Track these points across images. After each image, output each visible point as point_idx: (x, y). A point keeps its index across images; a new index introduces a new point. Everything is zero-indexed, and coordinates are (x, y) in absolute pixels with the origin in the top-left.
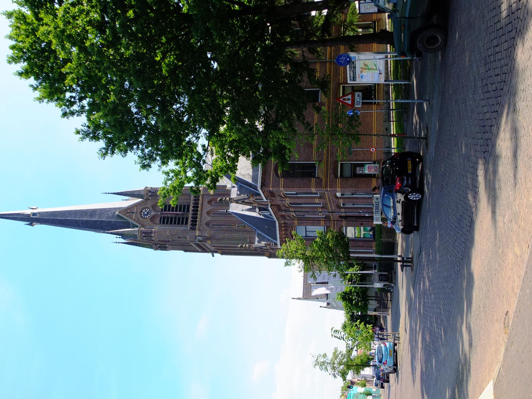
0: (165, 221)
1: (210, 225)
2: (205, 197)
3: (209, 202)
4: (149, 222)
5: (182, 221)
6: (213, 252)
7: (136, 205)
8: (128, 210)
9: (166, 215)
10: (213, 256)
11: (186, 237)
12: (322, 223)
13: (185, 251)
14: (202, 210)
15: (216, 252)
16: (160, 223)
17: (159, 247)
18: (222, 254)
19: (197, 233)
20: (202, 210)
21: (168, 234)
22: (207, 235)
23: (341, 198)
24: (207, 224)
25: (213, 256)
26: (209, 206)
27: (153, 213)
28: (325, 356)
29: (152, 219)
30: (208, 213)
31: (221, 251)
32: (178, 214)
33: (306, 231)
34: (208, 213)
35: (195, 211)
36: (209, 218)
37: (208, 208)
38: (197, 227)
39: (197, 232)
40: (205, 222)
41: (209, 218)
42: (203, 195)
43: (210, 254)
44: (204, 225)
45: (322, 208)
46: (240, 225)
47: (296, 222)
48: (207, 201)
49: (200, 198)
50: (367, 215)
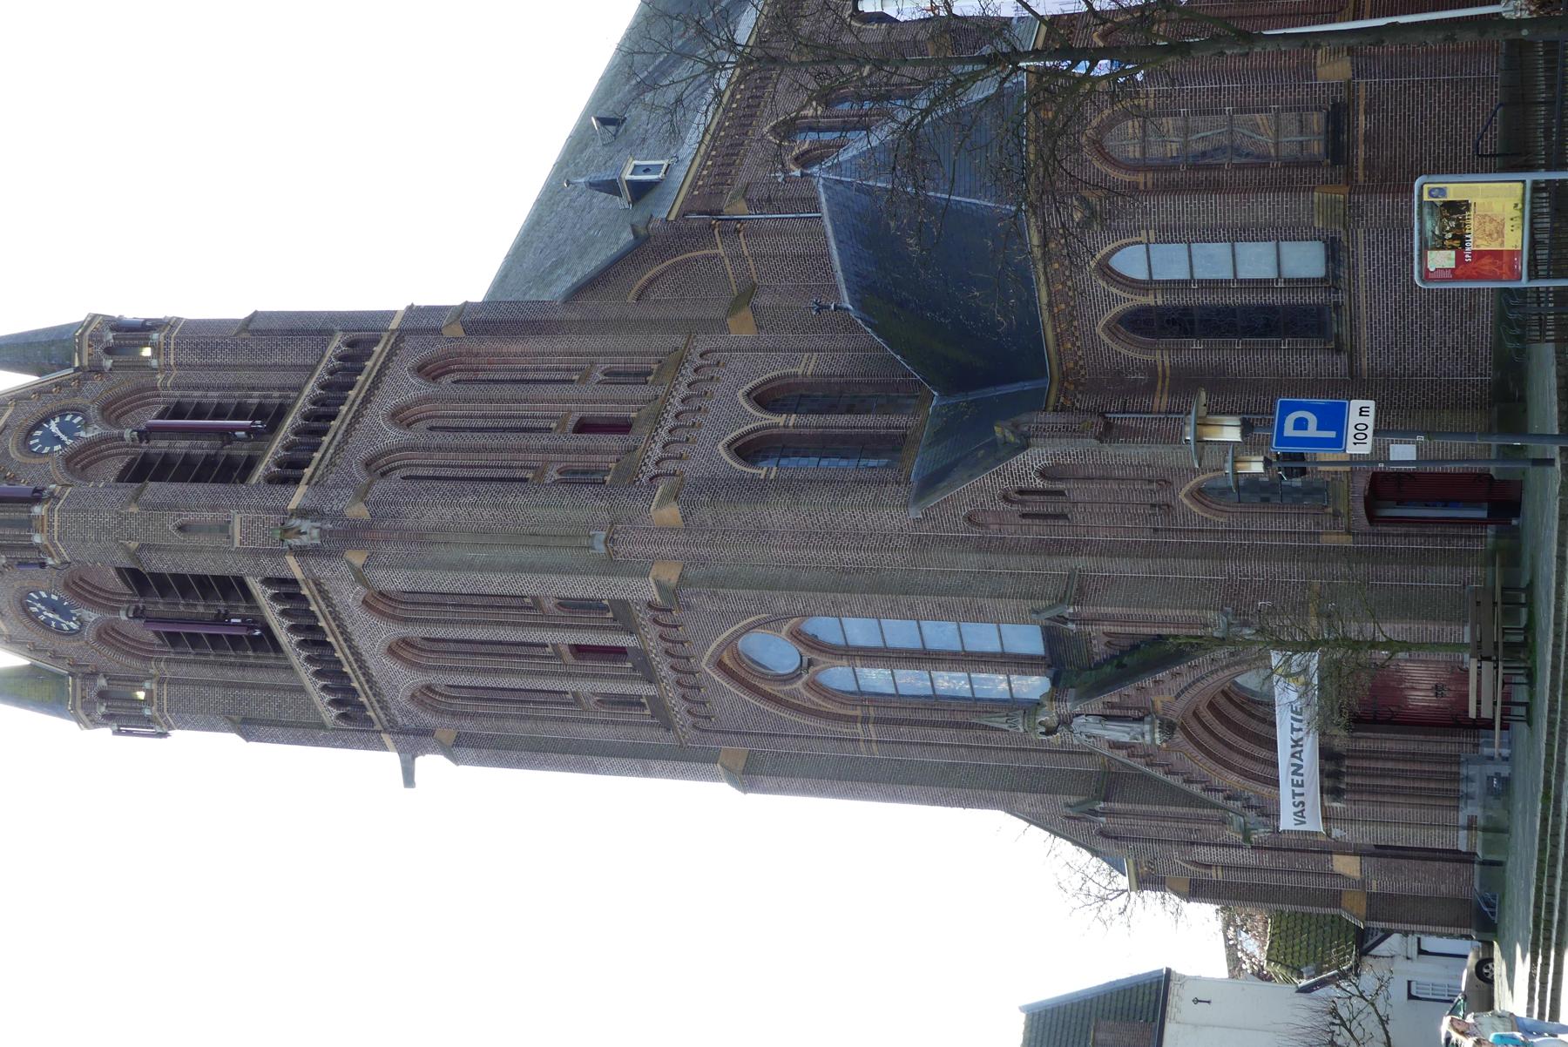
2: (410, 342)
3: (428, 371)
4: (55, 468)
10: (409, 779)
11: (224, 528)
14: (366, 401)
17: (103, 695)
24: (377, 466)
25: (409, 779)
30: (399, 417)
34: (399, 417)
37: (404, 387)
38: (308, 472)
39: (302, 489)
40: (364, 455)
41: (393, 436)
43: (389, 760)
48: (413, 361)
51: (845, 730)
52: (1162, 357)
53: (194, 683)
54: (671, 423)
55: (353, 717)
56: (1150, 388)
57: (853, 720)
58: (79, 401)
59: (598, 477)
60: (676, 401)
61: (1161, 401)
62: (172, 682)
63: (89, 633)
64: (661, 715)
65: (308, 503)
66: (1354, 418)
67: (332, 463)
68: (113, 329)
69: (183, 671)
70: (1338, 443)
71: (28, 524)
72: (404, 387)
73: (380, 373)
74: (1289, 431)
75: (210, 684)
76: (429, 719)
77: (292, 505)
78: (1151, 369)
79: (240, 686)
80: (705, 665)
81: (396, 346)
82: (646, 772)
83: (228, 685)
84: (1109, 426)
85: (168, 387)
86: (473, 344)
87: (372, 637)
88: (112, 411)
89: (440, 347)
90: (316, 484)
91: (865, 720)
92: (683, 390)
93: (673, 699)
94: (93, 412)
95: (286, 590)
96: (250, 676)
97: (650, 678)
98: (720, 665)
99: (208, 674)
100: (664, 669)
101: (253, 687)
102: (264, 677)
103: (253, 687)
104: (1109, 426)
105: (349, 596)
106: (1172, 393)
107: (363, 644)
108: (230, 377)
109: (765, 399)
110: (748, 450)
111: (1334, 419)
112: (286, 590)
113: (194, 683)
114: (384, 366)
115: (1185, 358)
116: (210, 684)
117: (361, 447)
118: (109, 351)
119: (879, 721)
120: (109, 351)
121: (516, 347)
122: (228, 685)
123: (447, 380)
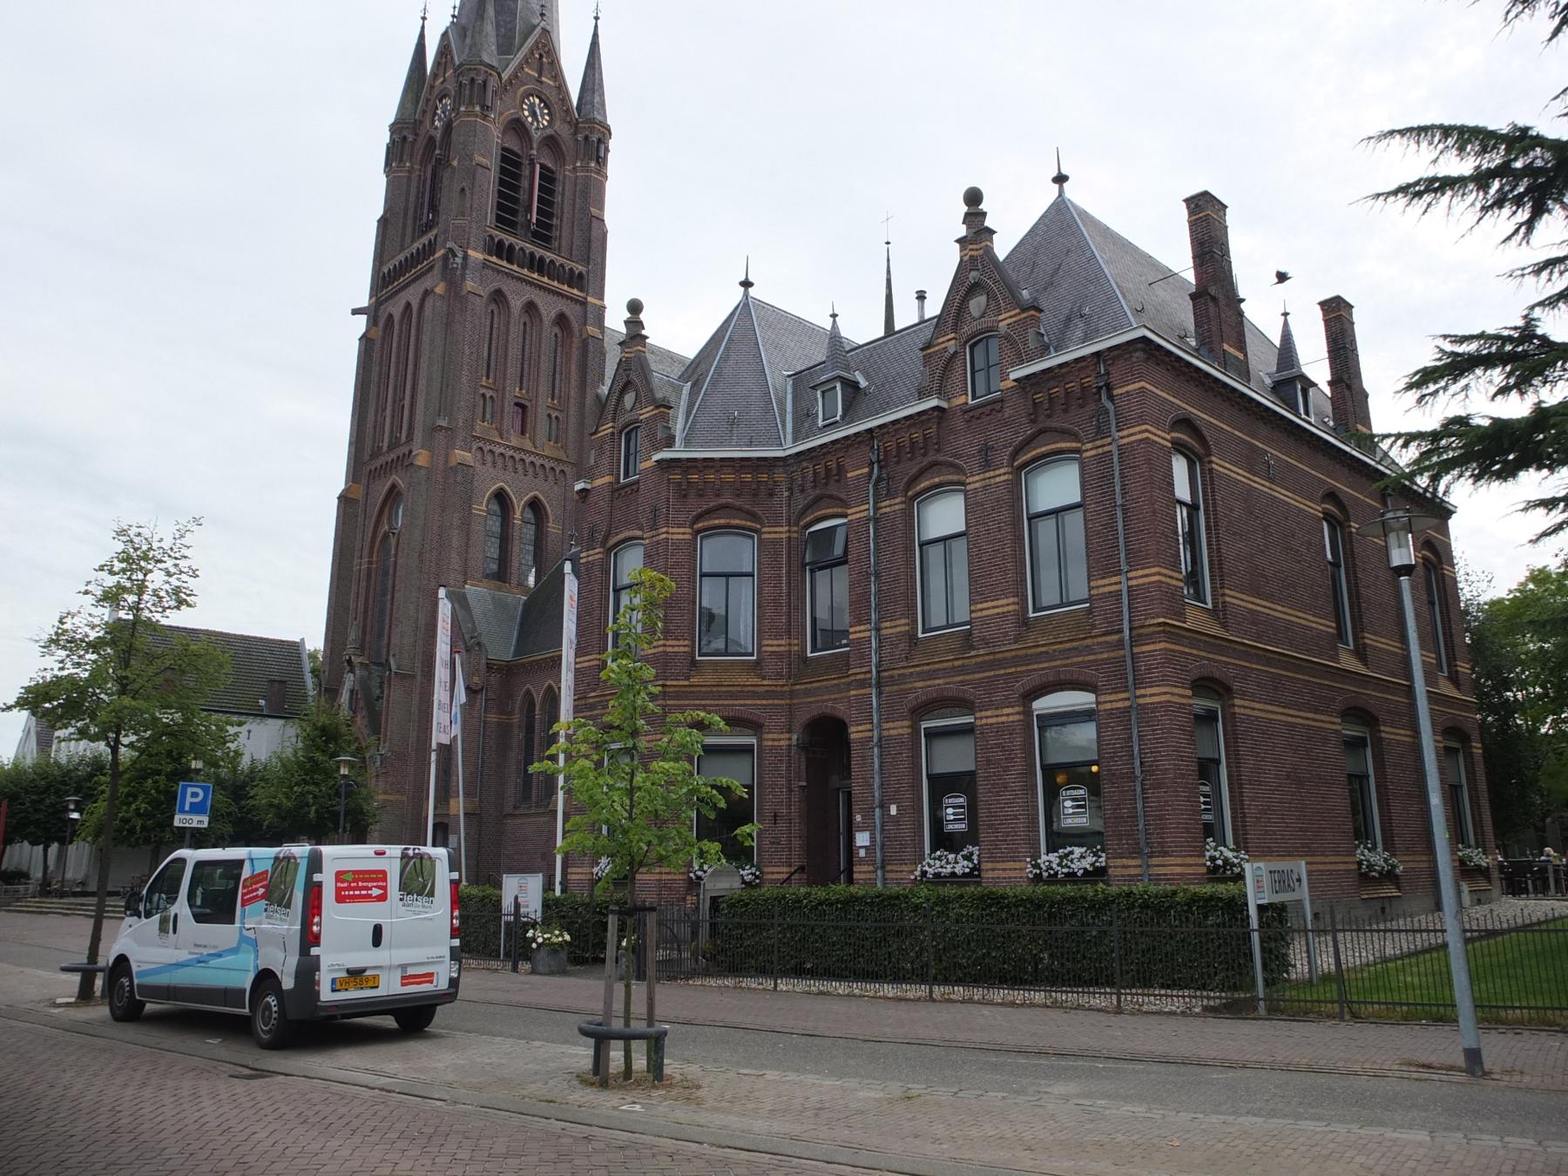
0: (510, 165)
1: (493, 306)
2: (578, 307)
3: (561, 320)
5: (507, 214)
6: (373, 312)
7: (561, 87)
8: (546, 56)
9: (526, 172)
10: (355, 312)
12: (775, 645)
13: (384, 223)
14: (541, 287)
15: (373, 322)
16: (504, 149)
18: (365, 339)
19: (476, 255)
20: (541, 287)
21: (479, 159)
22: (470, 285)
23: (1028, 712)
24: (498, 297)
25: (355, 312)
26: (553, 314)
27: (536, 136)
28: (181, 600)
29: (517, 127)
30: (530, 307)
31: (377, 333)
32: (529, 209)
33: (727, 575)
34: (530, 307)
35: (539, 265)
36: (516, 304)
37: (549, 309)
38: (494, 259)
39: (480, 256)
40: (504, 289)
41: (516, 304)
42: (584, 303)
43: (364, 301)
44: (495, 285)
45: (912, 637)
46: (489, 402)
47: (782, 532)
48: (568, 313)
49: (575, 291)
50: (862, 839)
51: (366, 552)
52: (516, 718)
53: (408, 191)
54: (517, 457)
55: (385, 280)
56: (502, 712)
57: (371, 556)
58: (558, 123)
59: (488, 416)
60: (532, 458)
61: (493, 718)
62: (409, 178)
63: (432, 132)
64: (375, 455)
65: (470, 261)
66: (196, 818)
67: (499, 272)
68: (600, 141)
69: (414, 184)
70: (182, 811)
71: (471, 103)
72: (549, 309)
73: (559, 294)
74: (190, 790)
75: (407, 200)
76: (381, 324)
77: (470, 252)
78: (511, 713)
79: (405, 215)
80: (394, 478)
81: (577, 301)
82: (351, 444)
83: (406, 210)
84: (476, 692)
85: (566, 173)
86: (576, 342)
87: (412, 295)
88: (551, 142)
89: (575, 326)
90: (485, 265)
91: (370, 563)
92: (539, 462)
93: (381, 460)
94: (549, 132)
95: (430, 248)
96: (410, 222)
97: (391, 448)
98: (394, 486)
99: (412, 199)
100: (393, 456)
101: (405, 224)
102: (409, 230)
103: (405, 224)
104: (476, 692)
105: (427, 282)
106: (499, 724)
107: (411, 289)
108: (567, 208)
109: (535, 505)
110: (501, 497)
111: (196, 809)
112: (430, 248)
113: (408, 195)
114: (563, 296)
115: (516, 731)
116: (407, 200)
117: (508, 287)
118: (586, 138)
119: (369, 570)
120: (586, 138)
121: (573, 367)
122: (406, 210)
123: (556, 330)
